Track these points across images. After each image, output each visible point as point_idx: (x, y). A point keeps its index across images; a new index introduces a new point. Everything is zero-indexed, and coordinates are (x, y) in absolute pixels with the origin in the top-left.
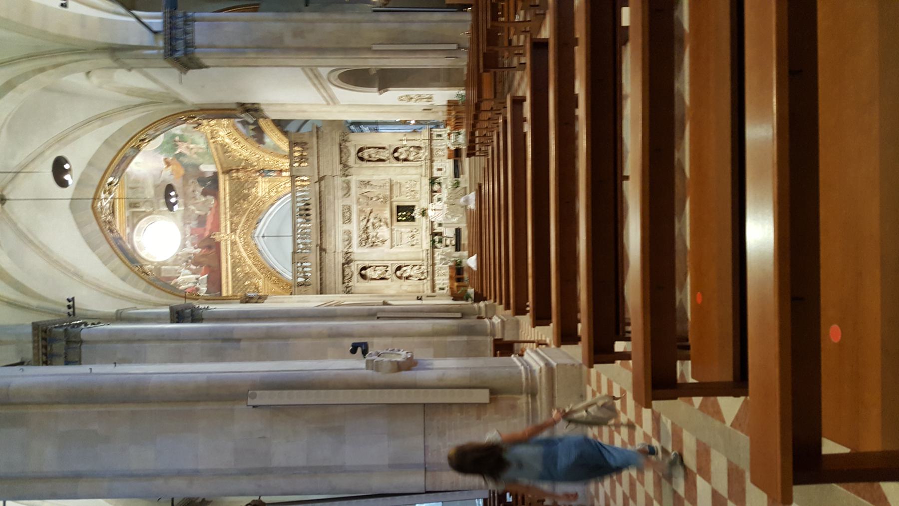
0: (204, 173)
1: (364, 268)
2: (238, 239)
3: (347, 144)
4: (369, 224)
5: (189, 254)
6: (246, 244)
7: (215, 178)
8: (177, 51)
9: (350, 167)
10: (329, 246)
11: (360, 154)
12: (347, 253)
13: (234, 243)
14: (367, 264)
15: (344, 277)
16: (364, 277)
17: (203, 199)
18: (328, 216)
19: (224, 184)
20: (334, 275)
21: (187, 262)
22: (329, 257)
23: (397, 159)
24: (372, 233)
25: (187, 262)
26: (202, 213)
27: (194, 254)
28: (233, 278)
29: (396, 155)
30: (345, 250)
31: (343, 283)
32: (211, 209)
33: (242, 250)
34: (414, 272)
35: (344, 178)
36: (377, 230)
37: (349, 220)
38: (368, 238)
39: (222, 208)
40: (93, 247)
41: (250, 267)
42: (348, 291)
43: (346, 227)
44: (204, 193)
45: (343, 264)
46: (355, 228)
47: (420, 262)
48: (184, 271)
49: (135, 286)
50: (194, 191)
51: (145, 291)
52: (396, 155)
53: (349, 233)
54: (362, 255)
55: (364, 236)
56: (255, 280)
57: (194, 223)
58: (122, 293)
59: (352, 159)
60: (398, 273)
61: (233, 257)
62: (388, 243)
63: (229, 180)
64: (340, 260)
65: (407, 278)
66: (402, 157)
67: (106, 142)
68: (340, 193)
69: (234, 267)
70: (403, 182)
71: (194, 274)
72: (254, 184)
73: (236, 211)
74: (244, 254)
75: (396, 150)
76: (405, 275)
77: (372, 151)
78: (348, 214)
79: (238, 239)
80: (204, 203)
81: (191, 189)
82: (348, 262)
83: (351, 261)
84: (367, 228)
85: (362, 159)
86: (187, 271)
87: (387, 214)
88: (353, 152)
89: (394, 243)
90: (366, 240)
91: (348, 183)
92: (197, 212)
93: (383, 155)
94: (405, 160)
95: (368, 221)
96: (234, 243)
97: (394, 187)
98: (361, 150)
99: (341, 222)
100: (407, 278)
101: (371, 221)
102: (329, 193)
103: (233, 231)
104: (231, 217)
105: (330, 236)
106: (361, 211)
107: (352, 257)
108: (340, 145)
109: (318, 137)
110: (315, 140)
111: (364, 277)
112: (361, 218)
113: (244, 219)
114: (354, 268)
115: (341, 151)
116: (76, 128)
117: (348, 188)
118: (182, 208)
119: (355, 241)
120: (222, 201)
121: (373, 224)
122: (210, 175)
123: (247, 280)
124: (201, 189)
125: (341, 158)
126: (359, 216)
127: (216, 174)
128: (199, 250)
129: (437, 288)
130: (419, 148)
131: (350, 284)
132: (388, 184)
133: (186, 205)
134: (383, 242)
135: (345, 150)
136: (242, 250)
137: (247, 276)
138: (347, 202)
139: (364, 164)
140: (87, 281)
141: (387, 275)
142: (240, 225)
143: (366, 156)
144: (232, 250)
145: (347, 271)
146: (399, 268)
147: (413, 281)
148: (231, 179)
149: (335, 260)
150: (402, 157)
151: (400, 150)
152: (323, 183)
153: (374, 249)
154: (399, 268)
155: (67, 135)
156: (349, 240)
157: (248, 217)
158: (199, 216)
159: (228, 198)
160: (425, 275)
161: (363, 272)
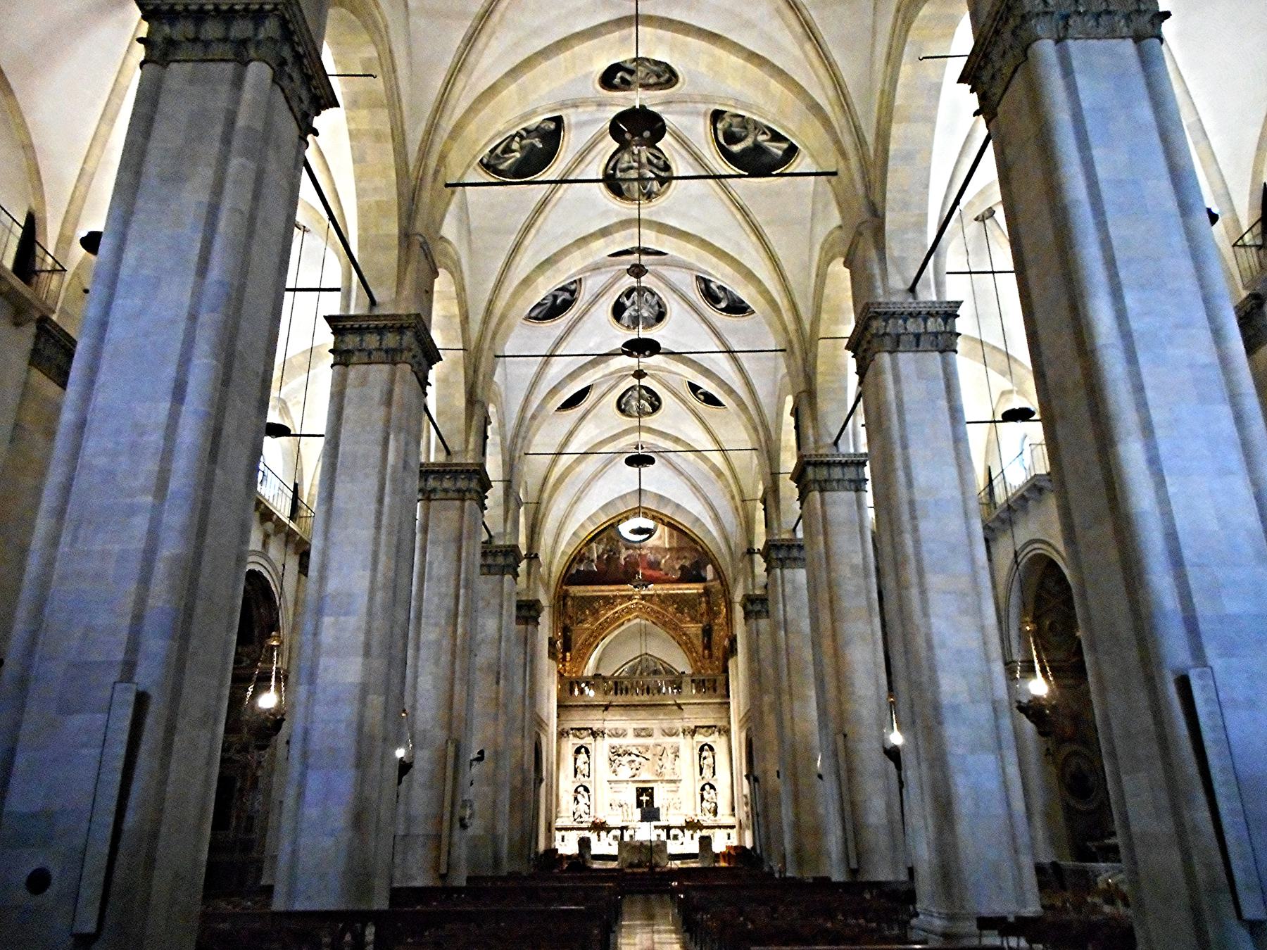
0: (705, 567)
1: (587, 752)
2: (634, 601)
3: (717, 734)
4: (633, 757)
5: (620, 552)
6: (629, 611)
7: (701, 579)
8: (752, 605)
9: (693, 736)
10: (609, 715)
11: (706, 747)
12: (603, 733)
13: (630, 598)
14: (592, 754)
15: (579, 729)
16: (578, 751)
17: (677, 567)
18: (642, 713)
19: (693, 589)
20: (577, 720)
21: (611, 551)
22: (598, 714)
23: (703, 789)
24: (626, 759)
25: (611, 551)
26: (662, 566)
27: (619, 558)
28: (594, 597)
29: (707, 787)
30: (606, 731)
31: (572, 729)
32: (667, 574)
33: (624, 606)
34: (582, 808)
35: (681, 730)
36: (627, 765)
37: (638, 735)
38: (619, 755)
39: (668, 586)
40: (604, 508)
41: (604, 615)
42: (562, 734)
43: (630, 732)
44: (682, 568)
45: (591, 729)
46: (629, 741)
47: (592, 814)
48: (601, 547)
49: (569, 544)
50: (685, 557)
51: (563, 553)
52: (707, 787)
53: (624, 735)
54: (601, 749)
55: (621, 752)
56: (590, 620)
57: (651, 557)
58: (562, 535)
59: (700, 738)
60: (581, 789)
61: (615, 596)
62: (613, 777)
63: (698, 593)
64: (596, 726)
65: (576, 799)
66: (705, 793)
67: (697, 520)
68: (666, 725)
69: (606, 599)
70: (678, 795)
71: (598, 557)
72: (693, 620)
73: (665, 600)
74: (618, 608)
75: (712, 787)
76: (579, 797)
77: (710, 760)
78: (643, 734)
79: (634, 601)
80: (673, 568)
81: (686, 554)
82: (594, 734)
83: (595, 737)
84: (630, 754)
85: (702, 749)
86: (601, 551)
87: (644, 775)
88: (709, 740)
89: (613, 785)
90: (616, 753)
91: (676, 734)
92: (663, 561)
93: (707, 772)
94: (703, 799)
95: (638, 756)
96: (630, 598)
97: (673, 785)
98: (711, 749)
99: (635, 726)
100: (576, 799)
101: (638, 760)
102: (665, 714)
103: (643, 597)
104: (659, 596)
105: (622, 715)
106: (647, 749)
107: (598, 738)
108: (715, 727)
109: (720, 704)
110: (718, 700)
111: (578, 751)
112: (640, 748)
113: (656, 608)
114: (588, 741)
115: (709, 727)
116: (706, 499)
117: (671, 733)
118: (667, 546)
119: (616, 742)
120: (675, 586)
121: (633, 761)
122: (703, 574)
123: (590, 611)
124: (687, 563)
125: (703, 727)
126: (642, 746)
127: (703, 580)
128: (623, 563)
129: (563, 833)
130: (715, 813)
131: (571, 736)
132: (674, 778)
133: (670, 549)
134: (614, 772)
135: (710, 731)
136: (624, 606)
137: (595, 613)
138: (657, 733)
139: (697, 751)
140: (572, 507)
141: (579, 776)
142: (648, 604)
143: (705, 754)
144: (623, 596)
145: (585, 733)
146: (586, 790)
147: (573, 806)
148: (700, 595)
149: (595, 720)
150: (705, 793)
151: (712, 791)
152: (675, 708)
153: (607, 762)
154: (586, 790)
155: (699, 492)
156: (617, 735)
157: (658, 612)
158: (659, 563)
159: (679, 592)
160: (579, 820)
161: (583, 750)
